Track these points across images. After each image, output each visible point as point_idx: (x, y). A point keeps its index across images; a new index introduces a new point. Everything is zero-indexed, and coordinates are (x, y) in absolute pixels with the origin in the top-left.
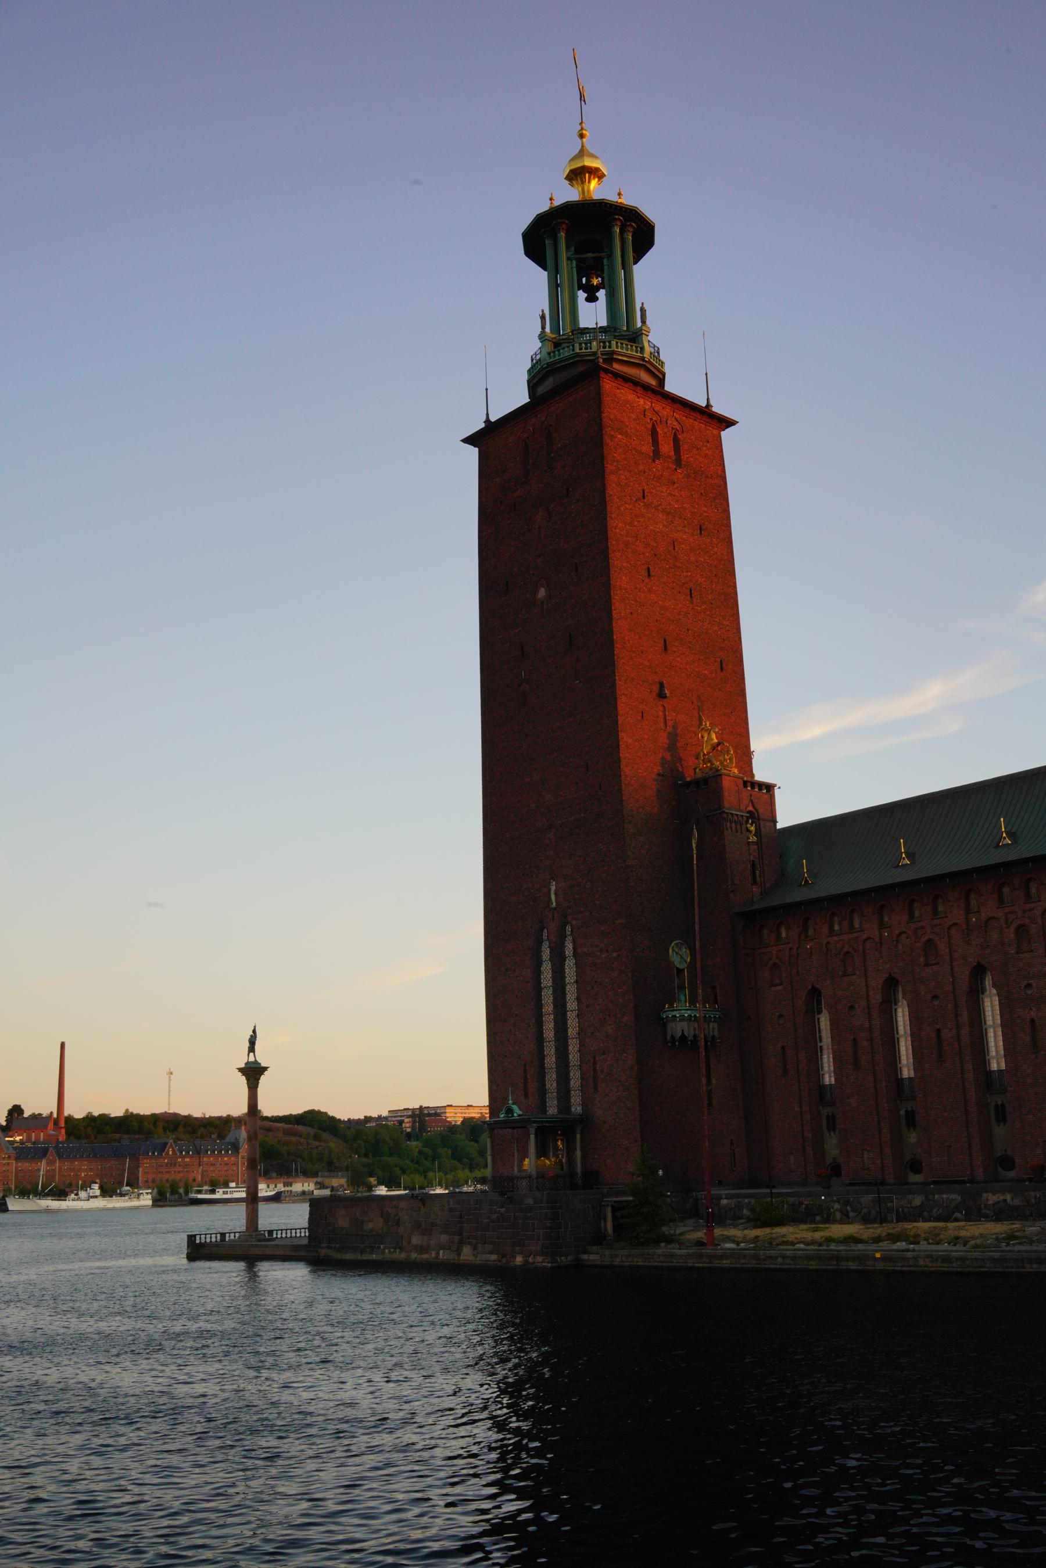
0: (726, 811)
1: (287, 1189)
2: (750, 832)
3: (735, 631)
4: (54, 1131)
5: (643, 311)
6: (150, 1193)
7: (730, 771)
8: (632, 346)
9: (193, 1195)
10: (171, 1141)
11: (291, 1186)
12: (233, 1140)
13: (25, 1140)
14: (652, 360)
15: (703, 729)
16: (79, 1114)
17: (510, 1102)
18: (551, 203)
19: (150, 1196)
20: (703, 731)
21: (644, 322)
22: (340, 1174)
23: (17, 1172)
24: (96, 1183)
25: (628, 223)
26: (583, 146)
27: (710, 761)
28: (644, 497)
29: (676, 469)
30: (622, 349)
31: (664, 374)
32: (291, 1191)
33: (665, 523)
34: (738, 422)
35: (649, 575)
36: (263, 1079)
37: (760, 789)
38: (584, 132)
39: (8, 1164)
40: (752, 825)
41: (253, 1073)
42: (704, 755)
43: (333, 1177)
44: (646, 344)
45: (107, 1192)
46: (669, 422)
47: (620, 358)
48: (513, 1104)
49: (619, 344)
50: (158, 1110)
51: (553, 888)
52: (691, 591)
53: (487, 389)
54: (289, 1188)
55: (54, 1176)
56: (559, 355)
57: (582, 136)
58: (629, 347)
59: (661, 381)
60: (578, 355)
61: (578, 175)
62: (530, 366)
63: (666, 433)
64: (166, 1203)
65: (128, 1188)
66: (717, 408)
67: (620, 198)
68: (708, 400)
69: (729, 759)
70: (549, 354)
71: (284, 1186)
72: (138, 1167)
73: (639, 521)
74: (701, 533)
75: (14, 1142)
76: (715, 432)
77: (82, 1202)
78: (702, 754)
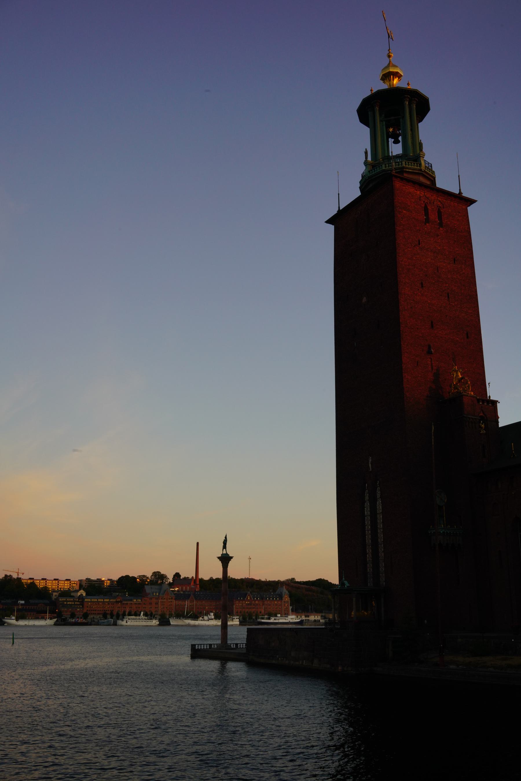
0: (465, 416)
1: (307, 618)
2: (482, 428)
3: (476, 316)
4: (194, 586)
5: (421, 145)
6: (239, 618)
7: (468, 393)
8: (414, 164)
9: (259, 620)
10: (249, 592)
11: (309, 617)
13: (180, 590)
14: (427, 171)
15: (453, 370)
16: (206, 578)
17: (343, 579)
18: (371, 93)
19: (238, 620)
20: (453, 372)
21: (421, 150)
24: (212, 612)
25: (413, 99)
26: (390, 62)
27: (457, 389)
28: (419, 244)
29: (439, 228)
30: (411, 166)
31: (434, 178)
32: (309, 620)
33: (432, 258)
34: (477, 201)
35: (422, 286)
36: (231, 564)
37: (488, 403)
38: (390, 54)
39: (172, 601)
40: (482, 424)
41: (225, 559)
42: (454, 385)
44: (423, 162)
46: (435, 203)
47: (408, 170)
48: (345, 580)
49: (407, 163)
51: (370, 460)
52: (448, 294)
53: (339, 194)
54: (308, 618)
55: (193, 608)
56: (375, 171)
57: (389, 56)
58: (413, 164)
59: (433, 181)
60: (384, 170)
61: (387, 76)
62: (361, 178)
63: (433, 209)
66: (465, 194)
67: (408, 86)
68: (460, 190)
69: (467, 387)
70: (369, 172)
71: (305, 617)
73: (416, 257)
74: (455, 262)
75: (175, 591)
76: (464, 207)
77: (206, 622)
78: (453, 384)
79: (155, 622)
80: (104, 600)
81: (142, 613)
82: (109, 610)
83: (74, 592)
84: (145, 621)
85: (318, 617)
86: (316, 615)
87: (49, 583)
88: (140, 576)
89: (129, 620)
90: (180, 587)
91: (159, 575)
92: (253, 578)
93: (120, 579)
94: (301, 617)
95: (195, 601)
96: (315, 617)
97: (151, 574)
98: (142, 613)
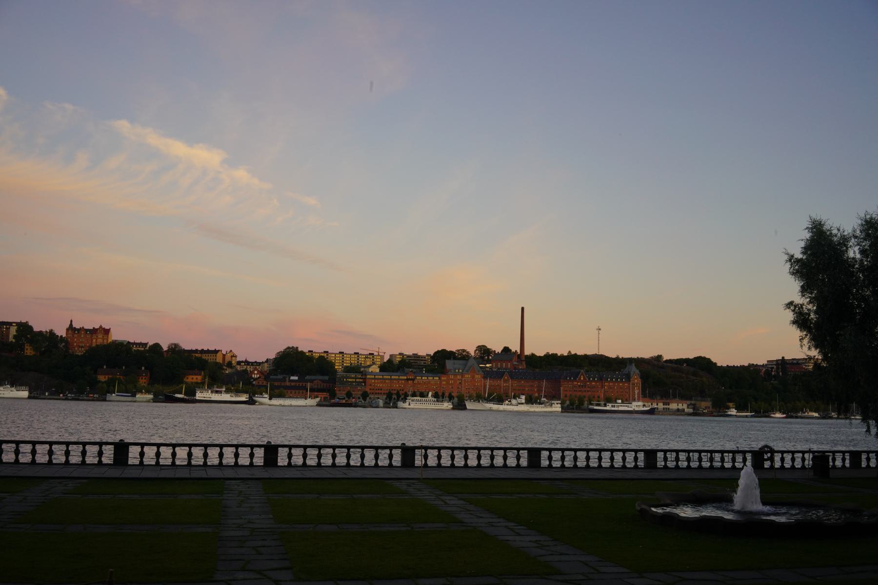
1: (665, 406)
4: (517, 362)
9: (591, 407)
11: (669, 405)
12: (627, 372)
16: (540, 353)
19: (559, 405)
22: (709, 399)
23: (503, 386)
24: (523, 395)
32: (669, 408)
43: (702, 401)
45: (530, 401)
50: (590, 352)
54: (667, 407)
64: (574, 411)
65: (545, 399)
71: (664, 405)
72: (561, 386)
79: (447, 405)
80: (391, 376)
81: (430, 394)
82: (395, 390)
83: (364, 367)
84: (434, 403)
85: (684, 405)
86: (681, 403)
87: (346, 357)
88: (458, 351)
89: (413, 402)
90: (494, 364)
91: (484, 350)
92: (603, 354)
93: (436, 353)
94: (652, 404)
95: (510, 380)
96: (678, 405)
97: (475, 349)
98: (430, 394)
